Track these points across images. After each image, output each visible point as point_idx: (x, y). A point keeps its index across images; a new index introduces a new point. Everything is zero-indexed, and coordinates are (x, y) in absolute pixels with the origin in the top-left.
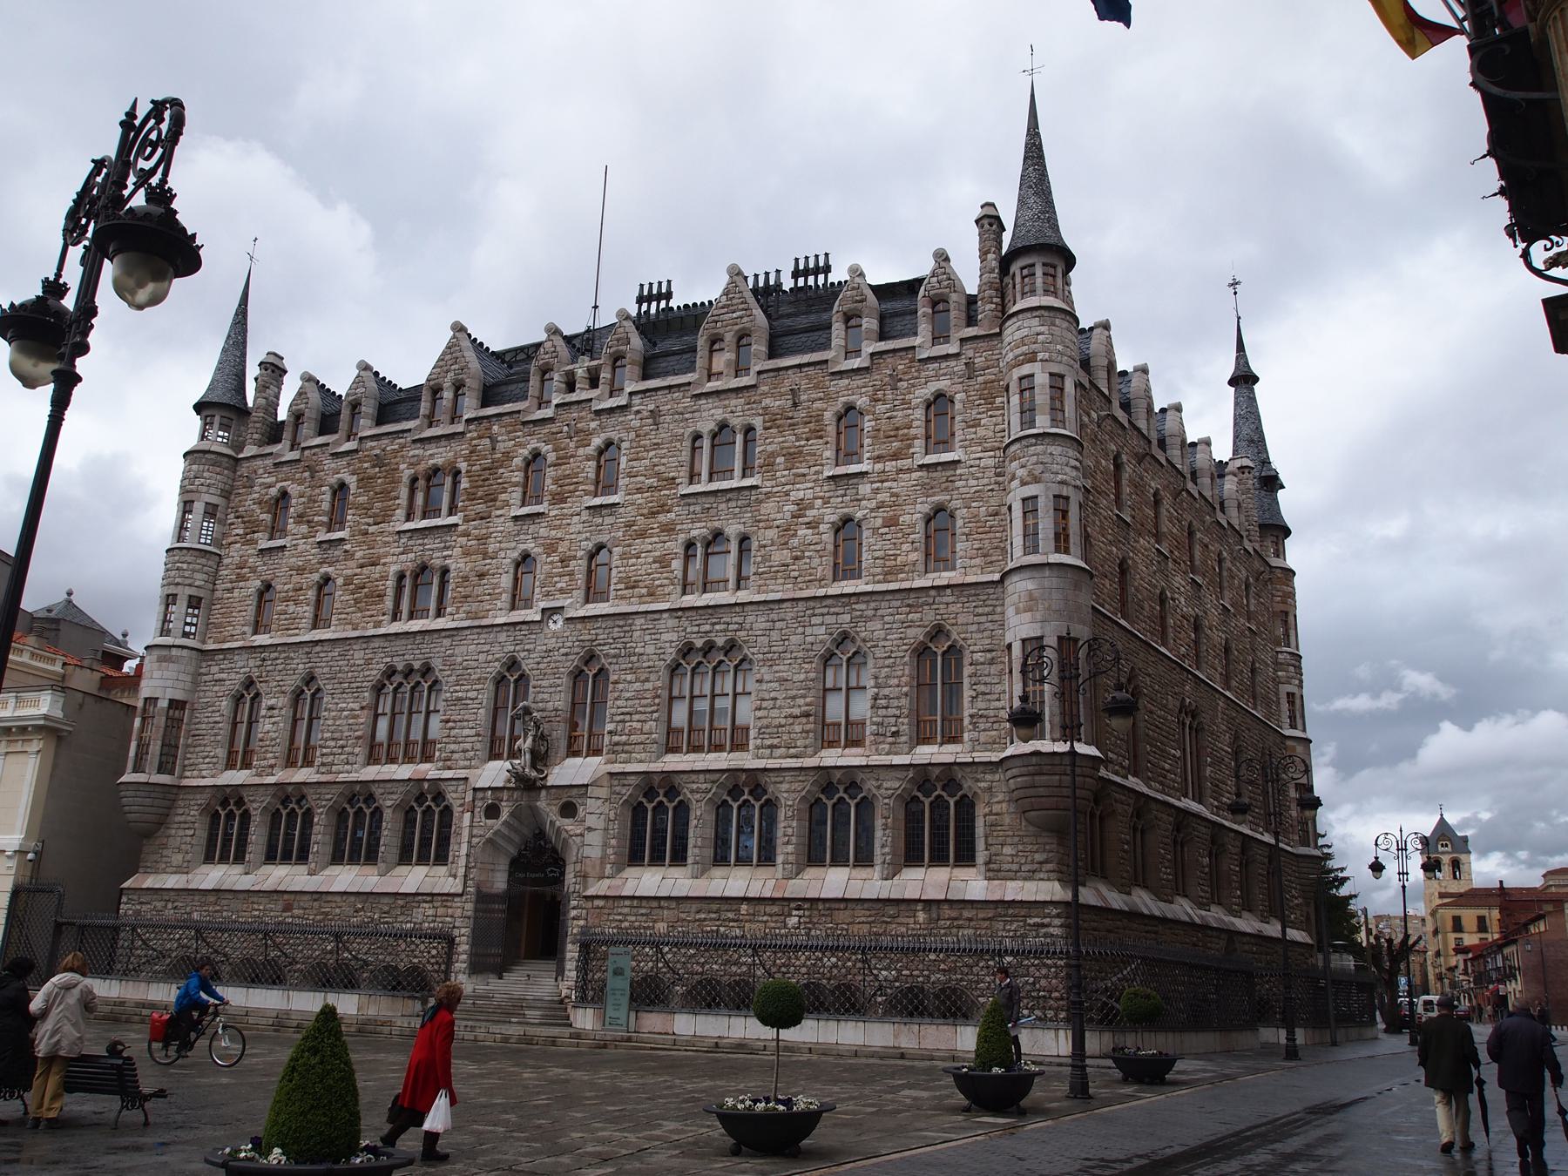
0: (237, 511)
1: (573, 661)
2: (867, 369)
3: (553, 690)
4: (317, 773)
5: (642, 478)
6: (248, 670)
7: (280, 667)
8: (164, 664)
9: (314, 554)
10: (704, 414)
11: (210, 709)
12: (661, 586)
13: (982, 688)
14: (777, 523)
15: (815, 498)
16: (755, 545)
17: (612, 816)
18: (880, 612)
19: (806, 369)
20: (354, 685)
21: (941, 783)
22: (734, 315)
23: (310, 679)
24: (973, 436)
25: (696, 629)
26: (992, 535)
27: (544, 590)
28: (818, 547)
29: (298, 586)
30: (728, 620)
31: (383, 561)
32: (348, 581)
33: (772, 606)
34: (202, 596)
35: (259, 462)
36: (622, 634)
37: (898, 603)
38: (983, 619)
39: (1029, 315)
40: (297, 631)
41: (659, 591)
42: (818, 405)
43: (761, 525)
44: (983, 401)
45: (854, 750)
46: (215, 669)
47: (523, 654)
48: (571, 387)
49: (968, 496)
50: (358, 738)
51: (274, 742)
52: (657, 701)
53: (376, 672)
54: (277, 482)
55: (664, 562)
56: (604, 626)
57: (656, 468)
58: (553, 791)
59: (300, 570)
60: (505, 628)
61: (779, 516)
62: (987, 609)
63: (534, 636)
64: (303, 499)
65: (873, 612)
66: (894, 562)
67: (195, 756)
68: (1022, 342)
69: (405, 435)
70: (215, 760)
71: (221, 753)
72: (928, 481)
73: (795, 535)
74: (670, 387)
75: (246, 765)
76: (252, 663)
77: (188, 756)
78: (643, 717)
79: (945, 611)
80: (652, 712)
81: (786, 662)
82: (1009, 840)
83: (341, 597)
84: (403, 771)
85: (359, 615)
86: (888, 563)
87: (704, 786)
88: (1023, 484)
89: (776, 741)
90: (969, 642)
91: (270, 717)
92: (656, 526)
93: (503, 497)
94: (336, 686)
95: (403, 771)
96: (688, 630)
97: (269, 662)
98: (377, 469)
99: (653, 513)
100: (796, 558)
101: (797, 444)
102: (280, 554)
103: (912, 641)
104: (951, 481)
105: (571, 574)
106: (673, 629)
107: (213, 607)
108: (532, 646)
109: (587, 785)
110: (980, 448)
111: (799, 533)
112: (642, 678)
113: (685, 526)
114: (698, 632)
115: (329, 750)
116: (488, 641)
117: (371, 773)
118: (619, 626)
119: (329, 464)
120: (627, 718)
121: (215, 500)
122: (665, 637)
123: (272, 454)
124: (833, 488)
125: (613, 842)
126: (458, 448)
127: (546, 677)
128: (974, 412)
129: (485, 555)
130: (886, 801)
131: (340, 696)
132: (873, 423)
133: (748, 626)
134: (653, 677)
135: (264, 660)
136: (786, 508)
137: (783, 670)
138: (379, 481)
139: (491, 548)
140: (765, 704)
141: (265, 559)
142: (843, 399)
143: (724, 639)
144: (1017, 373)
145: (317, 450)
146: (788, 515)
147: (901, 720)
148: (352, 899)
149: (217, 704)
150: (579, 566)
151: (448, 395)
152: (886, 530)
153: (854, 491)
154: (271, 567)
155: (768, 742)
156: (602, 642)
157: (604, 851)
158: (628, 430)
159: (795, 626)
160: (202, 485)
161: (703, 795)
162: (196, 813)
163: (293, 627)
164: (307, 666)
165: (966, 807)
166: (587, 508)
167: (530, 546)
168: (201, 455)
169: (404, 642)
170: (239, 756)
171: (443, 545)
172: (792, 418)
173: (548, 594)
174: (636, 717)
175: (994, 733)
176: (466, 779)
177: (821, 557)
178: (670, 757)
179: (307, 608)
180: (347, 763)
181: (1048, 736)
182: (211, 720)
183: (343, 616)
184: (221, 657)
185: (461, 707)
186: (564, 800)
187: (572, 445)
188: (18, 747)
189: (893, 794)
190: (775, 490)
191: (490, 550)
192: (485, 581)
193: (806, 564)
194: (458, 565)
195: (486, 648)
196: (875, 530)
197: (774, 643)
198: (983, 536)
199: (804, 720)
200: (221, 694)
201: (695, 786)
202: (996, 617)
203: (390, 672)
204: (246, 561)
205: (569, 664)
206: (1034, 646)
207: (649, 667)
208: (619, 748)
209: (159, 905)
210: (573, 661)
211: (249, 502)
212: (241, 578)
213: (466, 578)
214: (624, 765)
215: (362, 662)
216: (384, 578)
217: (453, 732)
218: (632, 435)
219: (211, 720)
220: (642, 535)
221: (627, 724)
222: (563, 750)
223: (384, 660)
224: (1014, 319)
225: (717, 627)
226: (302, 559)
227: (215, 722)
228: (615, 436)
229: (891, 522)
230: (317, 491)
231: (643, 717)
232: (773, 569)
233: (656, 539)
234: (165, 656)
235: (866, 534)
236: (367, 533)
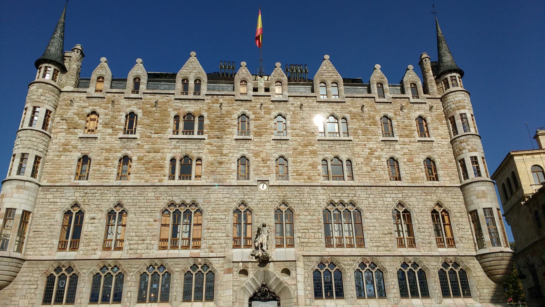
0: (62, 117)
1: (275, 204)
2: (391, 103)
3: (266, 217)
4: (127, 253)
5: (299, 131)
6: (75, 198)
7: (98, 198)
8: (20, 190)
9: (117, 144)
10: (323, 109)
11: (47, 218)
12: (313, 176)
13: (461, 227)
14: (364, 156)
15: (377, 148)
16: (354, 164)
17: (307, 276)
18: (414, 194)
19: (365, 99)
20: (148, 209)
21: (451, 264)
22: (330, 74)
23: (119, 204)
24: (437, 133)
25: (334, 195)
26: (451, 169)
27: (255, 172)
28: (382, 167)
29: (107, 158)
30: (349, 192)
31: (162, 151)
32: (140, 159)
33: (367, 188)
34: (41, 156)
35: (76, 95)
36: (299, 195)
37: (421, 192)
38: (455, 200)
39: (460, 92)
40: (108, 180)
41: (313, 178)
42: (372, 113)
43: (356, 156)
44: (438, 121)
45: (412, 249)
46: (51, 196)
47: (248, 200)
48: (255, 90)
49: (439, 154)
50: (154, 236)
51: (95, 237)
52: (320, 224)
53: (162, 204)
54: (90, 106)
55: (314, 166)
56: (289, 190)
57: (305, 128)
58: (277, 263)
59: (109, 150)
60: (238, 187)
61: (363, 153)
62: (457, 197)
63: (254, 192)
64: (108, 117)
65: (411, 194)
66: (414, 176)
67: (35, 243)
68: (460, 101)
69: (170, 95)
70: (50, 246)
71: (56, 242)
72: (422, 147)
73: (371, 161)
74: (306, 97)
76: (77, 194)
77: (31, 243)
78: (314, 231)
79: (440, 196)
80: (319, 229)
81: (377, 211)
82: (486, 287)
83: (134, 165)
85: (149, 175)
86: (412, 176)
87: (350, 263)
88: (470, 151)
89: (378, 244)
90: (452, 208)
91: (92, 223)
92: (308, 151)
93: (229, 130)
94: (137, 209)
96: (331, 195)
97: (90, 195)
98: (155, 109)
99: (306, 145)
100: (373, 170)
101: (366, 126)
102: (94, 141)
103: (429, 207)
104: (432, 148)
105: (268, 167)
106: (323, 194)
107: (46, 163)
108: (253, 197)
109: (295, 261)
110: (440, 138)
111: (373, 160)
112: (311, 214)
113: (321, 152)
114: (336, 196)
115: (135, 242)
116: (228, 192)
117: (163, 253)
118: (297, 191)
120: (306, 231)
121: (51, 109)
122: (320, 197)
123: (86, 92)
124: (384, 145)
125: (309, 288)
126: (201, 106)
127: (263, 211)
128: (436, 124)
129: (222, 154)
130: (433, 270)
131: (140, 214)
132: (396, 123)
133: (358, 196)
134: (317, 214)
135: (86, 193)
136: (365, 150)
137: (376, 214)
138: (156, 114)
139: (224, 152)
140: (371, 228)
141: (82, 142)
142: (384, 113)
143: (348, 200)
144: (458, 112)
145: (115, 94)
146: (368, 154)
147: (431, 237)
149: (52, 215)
150: (272, 163)
151: (192, 83)
152: (409, 163)
153: (394, 147)
154: (88, 147)
155: (375, 244)
156: (289, 197)
157: (305, 292)
158: (289, 110)
159: (379, 197)
160: (45, 100)
161: (350, 266)
162: (38, 275)
163: (104, 178)
164: (116, 198)
165: (463, 273)
166: (273, 140)
167: (246, 153)
168: (45, 85)
169: (179, 189)
171: (197, 147)
172: (362, 116)
173: (257, 174)
174: (312, 231)
175: (468, 244)
176: (224, 257)
177: (384, 171)
178: (328, 249)
179: (115, 169)
180: (147, 249)
181: (502, 245)
182: (47, 223)
183: (138, 175)
184: (55, 190)
185: (216, 222)
186: (283, 268)
187: (262, 113)
189: (435, 268)
190: (360, 143)
191: (224, 152)
192: (223, 166)
193: (378, 173)
194: (207, 158)
195: (228, 196)
196: (405, 163)
197: (371, 203)
198: (448, 169)
199: (389, 236)
200: (55, 210)
201: (346, 263)
202: (460, 200)
203: (172, 204)
204: (70, 142)
205: (273, 206)
207: (314, 209)
208: (305, 244)
210: (275, 204)
212: (65, 150)
213: (212, 164)
214: (309, 252)
215: (154, 198)
216: (164, 159)
217: (212, 234)
218: (292, 113)
219: (47, 223)
220: (301, 153)
221: (307, 234)
222: (274, 246)
223: (168, 198)
224: (454, 93)
225: (344, 195)
226: (109, 145)
227: (51, 225)
228: (283, 112)
229: (410, 161)
230: (117, 114)
231: (314, 231)
232: (364, 174)
233: (309, 156)
234: (21, 186)
235: (401, 164)
236: (150, 137)
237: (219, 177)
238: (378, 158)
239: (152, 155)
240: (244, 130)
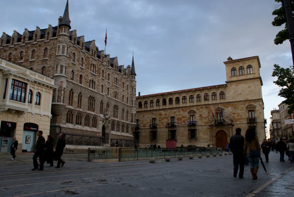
9: (80, 69)
32: (84, 78)
75: (72, 105)
83: (83, 79)
84: (93, 113)
95: (93, 113)
119: (81, 53)
135: (74, 86)
148: (90, 132)
150: (107, 89)
151: (94, 52)
167: (103, 84)
170: (71, 103)
188: (48, 91)
191: (100, 82)
194: (97, 83)
206: (135, 114)
209: (64, 130)
211: (69, 50)
216: (88, 79)
220: (111, 88)
228: (110, 73)
230: (80, 57)
237: (98, 90)
238: (122, 94)
239: (87, 77)
240: (103, 76)
